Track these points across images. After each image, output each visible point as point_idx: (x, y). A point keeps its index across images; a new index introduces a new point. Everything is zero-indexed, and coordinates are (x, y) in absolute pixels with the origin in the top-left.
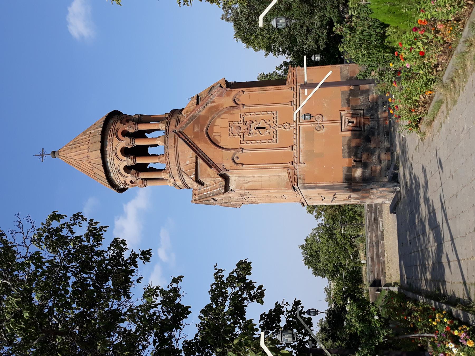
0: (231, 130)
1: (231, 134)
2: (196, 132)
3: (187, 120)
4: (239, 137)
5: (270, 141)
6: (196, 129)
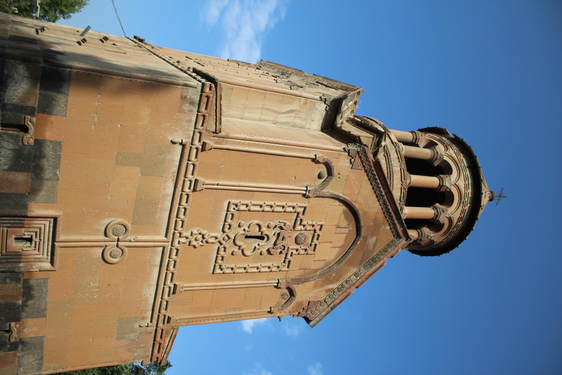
0: (316, 237)
1: (318, 228)
2: (374, 235)
3: (383, 259)
5: (243, 208)
6: (372, 240)
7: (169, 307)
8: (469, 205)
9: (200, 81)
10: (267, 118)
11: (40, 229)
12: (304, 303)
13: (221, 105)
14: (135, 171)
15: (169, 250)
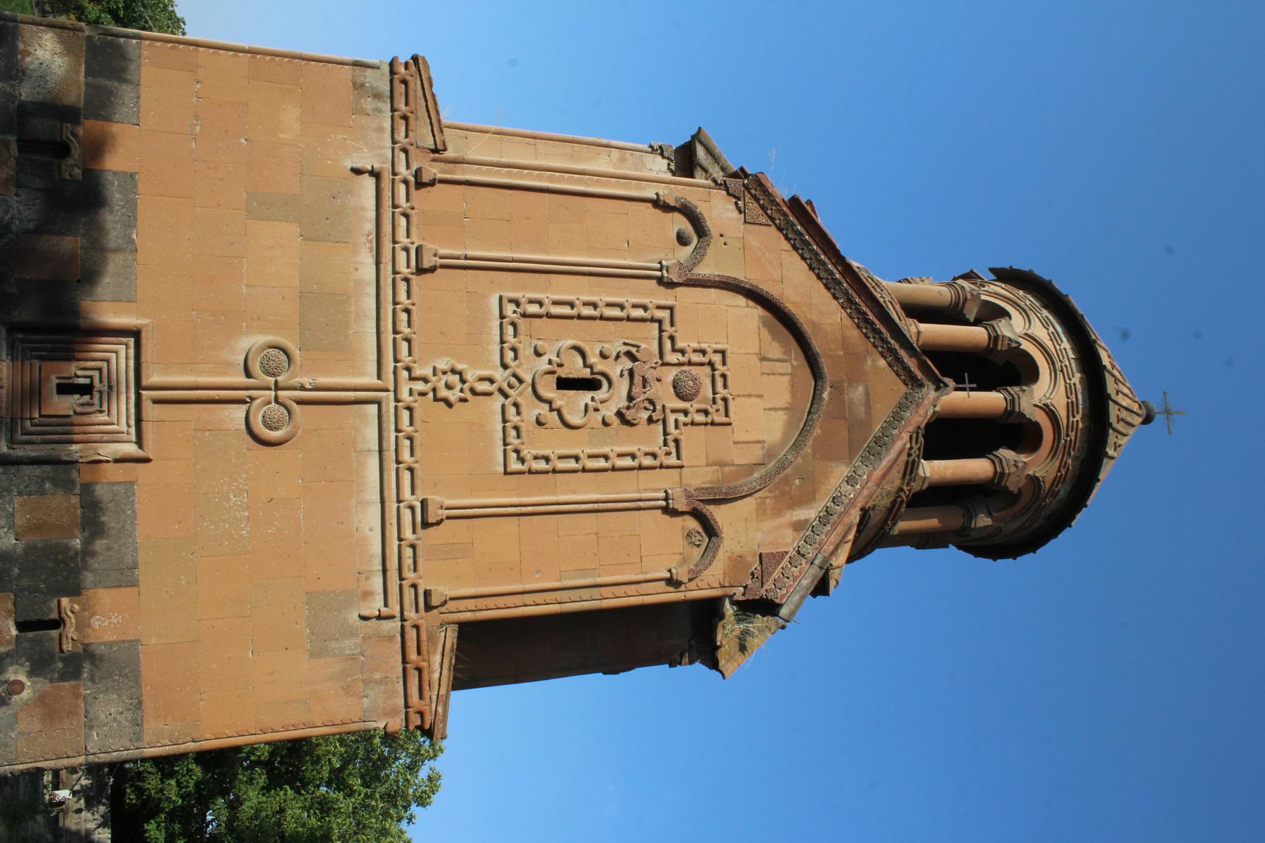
1: (717, 358)
3: (899, 436)
4: (680, 345)
5: (534, 309)
6: (857, 394)
7: (420, 561)
11: (108, 361)
12: (750, 559)
13: (433, 95)
14: (289, 231)
15: (392, 411)
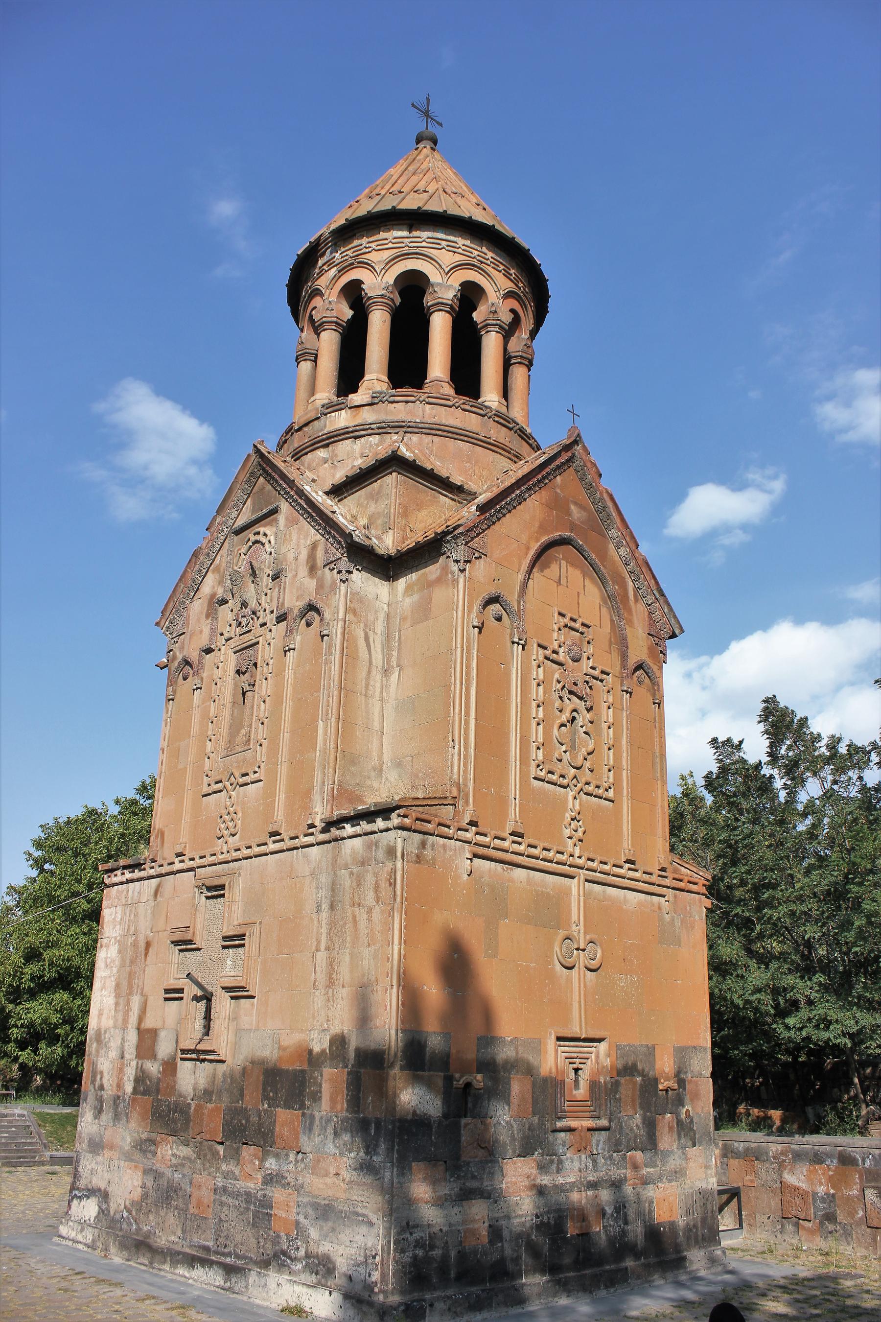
0: (572, 624)
2: (569, 508)
3: (601, 493)
5: (540, 753)
6: (576, 513)
7: (649, 870)
8: (484, 249)
9: (387, 830)
10: (378, 685)
